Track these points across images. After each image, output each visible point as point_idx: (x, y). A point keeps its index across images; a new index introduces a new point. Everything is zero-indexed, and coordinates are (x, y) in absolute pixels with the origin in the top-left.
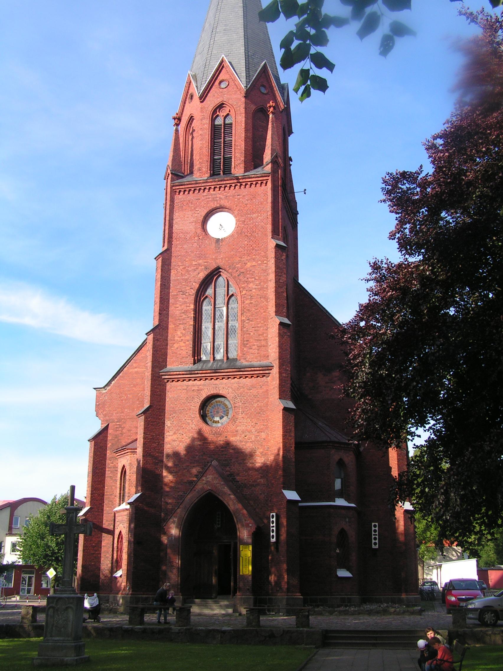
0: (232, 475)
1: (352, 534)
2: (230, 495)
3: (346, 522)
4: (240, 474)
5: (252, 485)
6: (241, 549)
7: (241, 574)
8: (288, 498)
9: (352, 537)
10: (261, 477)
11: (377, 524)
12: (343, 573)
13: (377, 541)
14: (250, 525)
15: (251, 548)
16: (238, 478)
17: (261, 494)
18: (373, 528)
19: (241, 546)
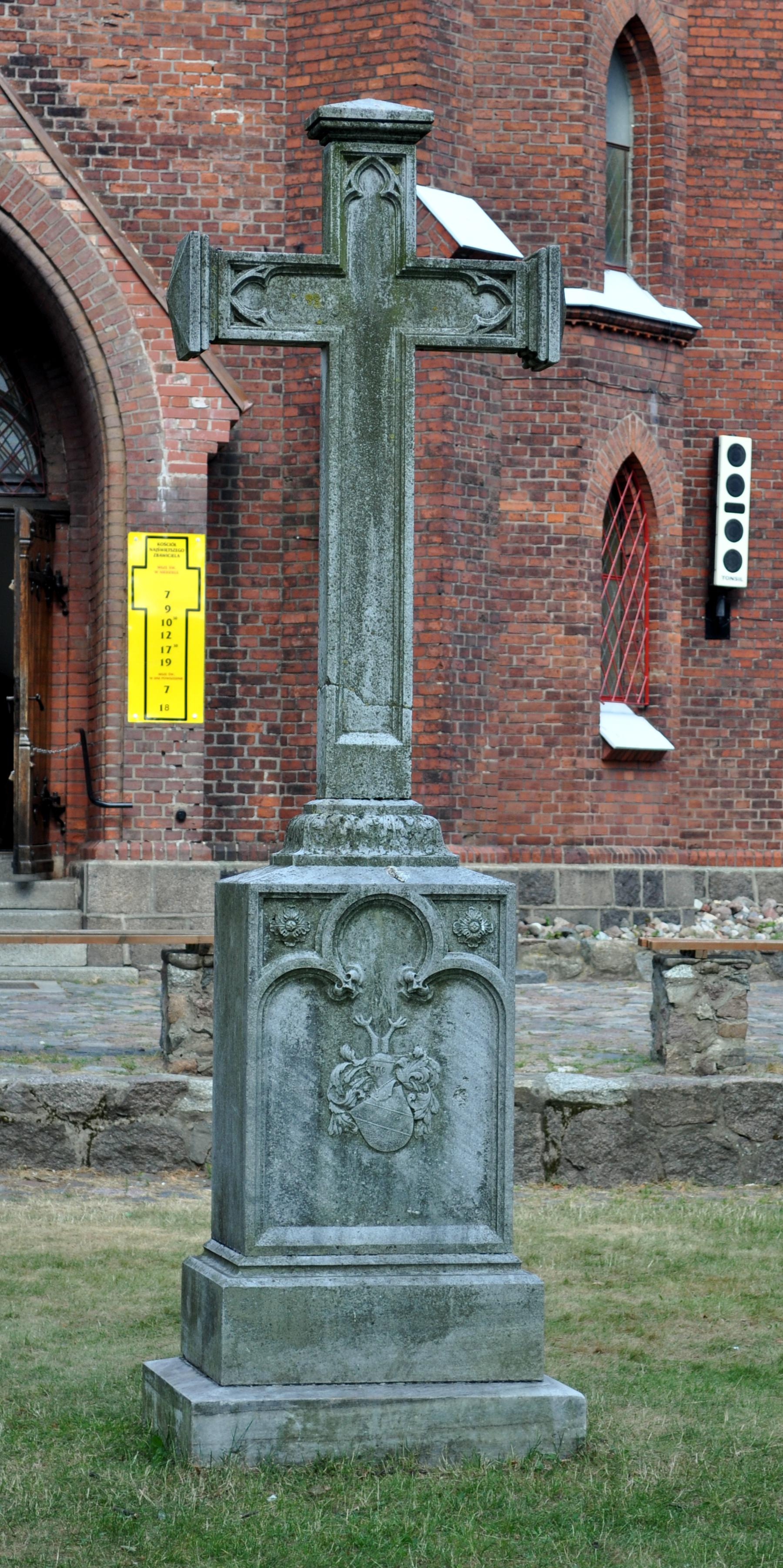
0: (41, 61)
1: (668, 488)
2: (56, 194)
3: (648, 419)
4: (93, 63)
5: (170, 143)
6: (135, 556)
7: (135, 715)
8: (464, 241)
9: (670, 511)
10: (239, 94)
11: (746, 443)
12: (624, 728)
13: (742, 546)
14: (198, 402)
15: (198, 542)
16: (74, 89)
17: (231, 204)
18: (726, 470)
19: (136, 542)
